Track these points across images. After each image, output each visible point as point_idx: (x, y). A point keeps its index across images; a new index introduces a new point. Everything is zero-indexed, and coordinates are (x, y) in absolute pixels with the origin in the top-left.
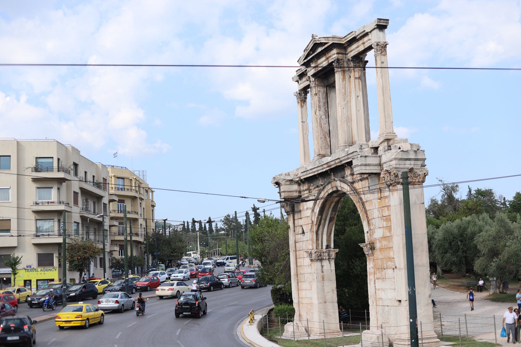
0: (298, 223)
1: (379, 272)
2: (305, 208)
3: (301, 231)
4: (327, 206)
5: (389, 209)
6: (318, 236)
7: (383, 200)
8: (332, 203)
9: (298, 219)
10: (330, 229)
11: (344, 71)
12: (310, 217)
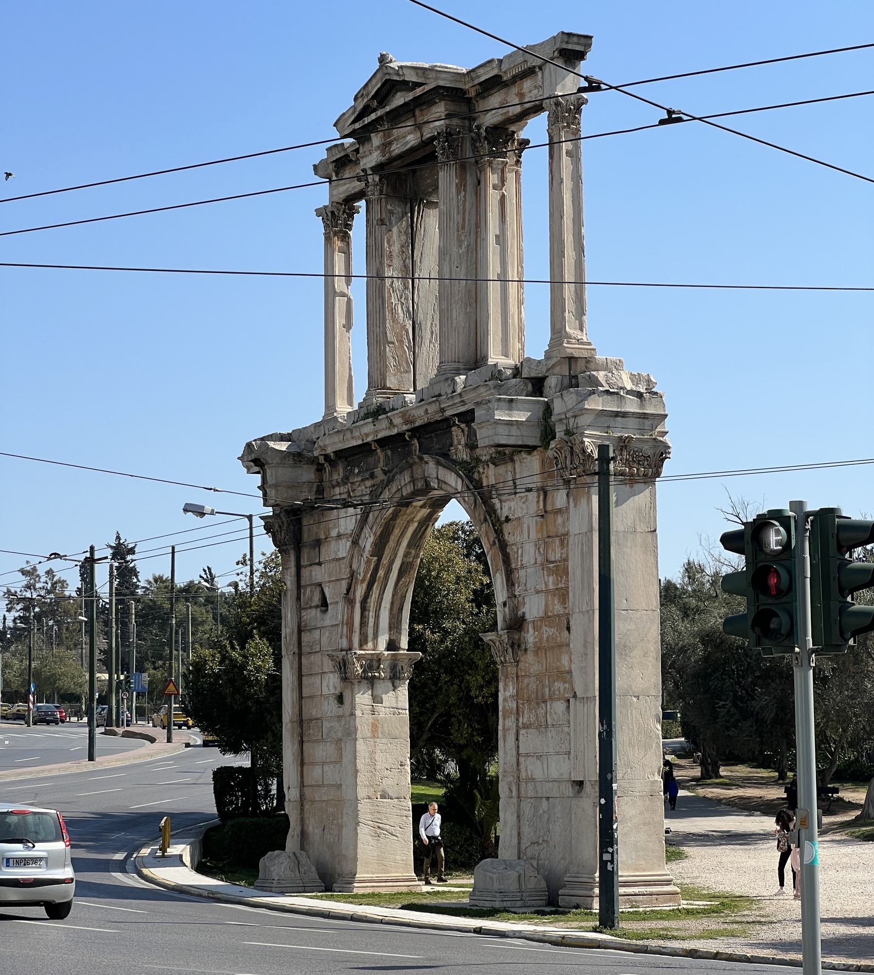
0: (311, 575)
1: (530, 710)
2: (334, 533)
3: (316, 600)
4: (397, 532)
5: (566, 541)
6: (367, 613)
7: (550, 518)
8: (412, 521)
9: (311, 565)
10: (399, 594)
11: (463, 168)
12: (347, 561)
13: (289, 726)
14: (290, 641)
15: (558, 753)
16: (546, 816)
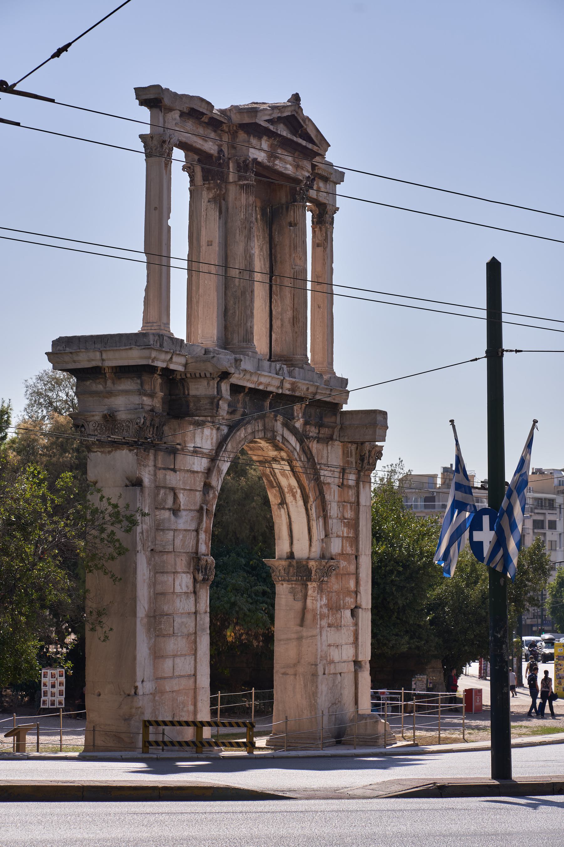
0: (165, 479)
1: (333, 615)
9: (164, 469)
13: (145, 620)
14: (147, 537)
15: (346, 644)
16: (340, 685)
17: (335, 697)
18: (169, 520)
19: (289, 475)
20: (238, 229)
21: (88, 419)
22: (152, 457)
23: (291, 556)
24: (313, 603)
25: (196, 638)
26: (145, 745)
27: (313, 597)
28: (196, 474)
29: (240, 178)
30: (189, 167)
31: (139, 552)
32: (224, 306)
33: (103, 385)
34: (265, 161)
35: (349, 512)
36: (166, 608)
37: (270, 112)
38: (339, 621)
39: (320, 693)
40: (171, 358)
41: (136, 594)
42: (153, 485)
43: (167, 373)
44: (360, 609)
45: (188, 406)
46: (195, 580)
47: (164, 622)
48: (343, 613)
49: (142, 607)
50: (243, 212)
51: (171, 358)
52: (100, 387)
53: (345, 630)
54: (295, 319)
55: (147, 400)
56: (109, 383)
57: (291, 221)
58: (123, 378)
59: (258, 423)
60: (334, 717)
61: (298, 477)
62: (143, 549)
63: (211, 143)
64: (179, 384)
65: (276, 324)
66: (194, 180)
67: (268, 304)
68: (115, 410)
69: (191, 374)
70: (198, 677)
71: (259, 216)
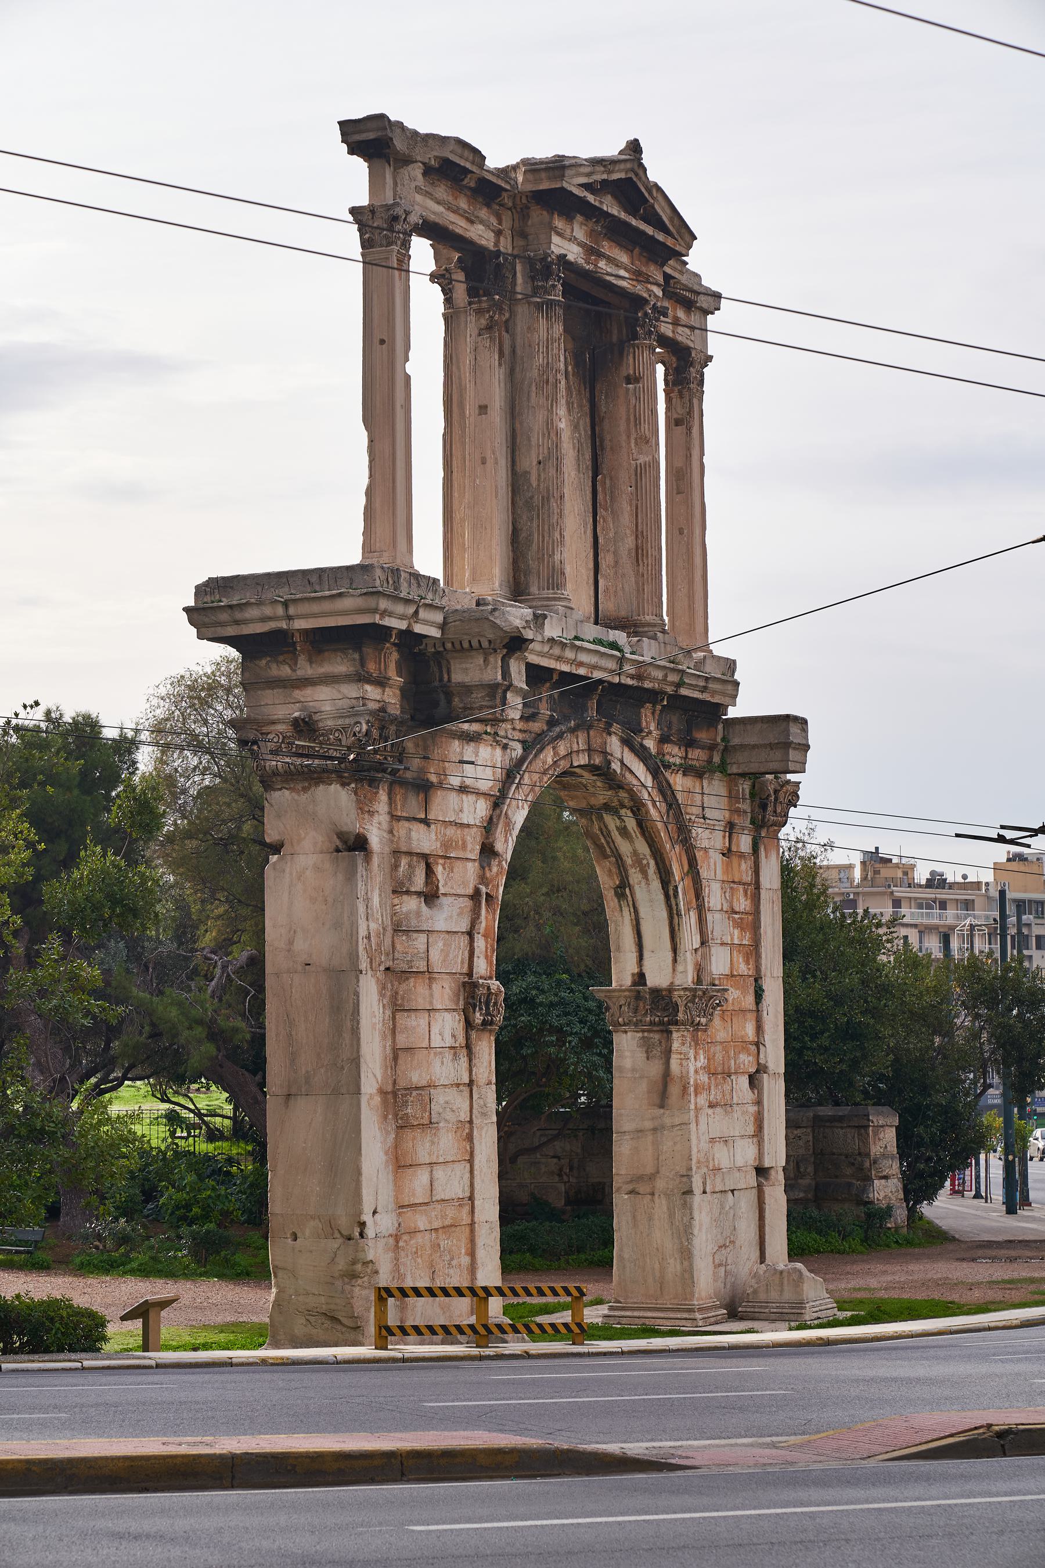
0: (409, 838)
13: (378, 1099)
14: (379, 945)
16: (732, 1212)
17: (724, 1234)
18: (418, 914)
19: (633, 834)
20: (534, 384)
21: (265, 729)
22: (383, 796)
23: (640, 978)
24: (681, 1064)
25: (471, 1129)
26: (380, 1334)
27: (681, 1053)
28: (466, 830)
29: (536, 290)
30: (443, 276)
31: (364, 972)
32: (510, 524)
33: (290, 666)
34: (581, 261)
35: (742, 900)
36: (416, 1077)
37: (587, 170)
38: (728, 1097)
39: (697, 1228)
40: (416, 612)
41: (358, 1051)
42: (387, 850)
43: (409, 640)
44: (765, 1075)
45: (449, 702)
46: (469, 1024)
47: (412, 1102)
48: (734, 1082)
49: (370, 1075)
50: (543, 353)
51: (416, 612)
52: (285, 671)
53: (739, 1113)
54: (640, 551)
55: (372, 692)
56: (302, 661)
57: (629, 375)
58: (328, 650)
59: (577, 738)
60: (723, 1269)
61: (652, 838)
62: (371, 968)
63: (481, 227)
64: (432, 663)
65: (606, 560)
66: (451, 297)
67: (590, 526)
68: (315, 711)
69: (453, 643)
70: (476, 1203)
71: (570, 368)
